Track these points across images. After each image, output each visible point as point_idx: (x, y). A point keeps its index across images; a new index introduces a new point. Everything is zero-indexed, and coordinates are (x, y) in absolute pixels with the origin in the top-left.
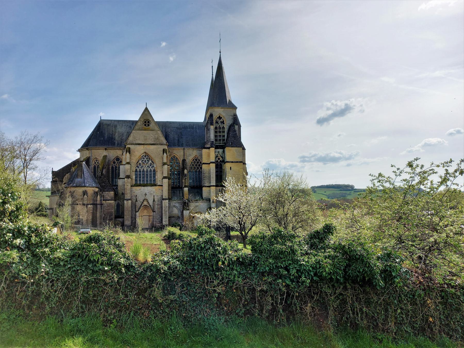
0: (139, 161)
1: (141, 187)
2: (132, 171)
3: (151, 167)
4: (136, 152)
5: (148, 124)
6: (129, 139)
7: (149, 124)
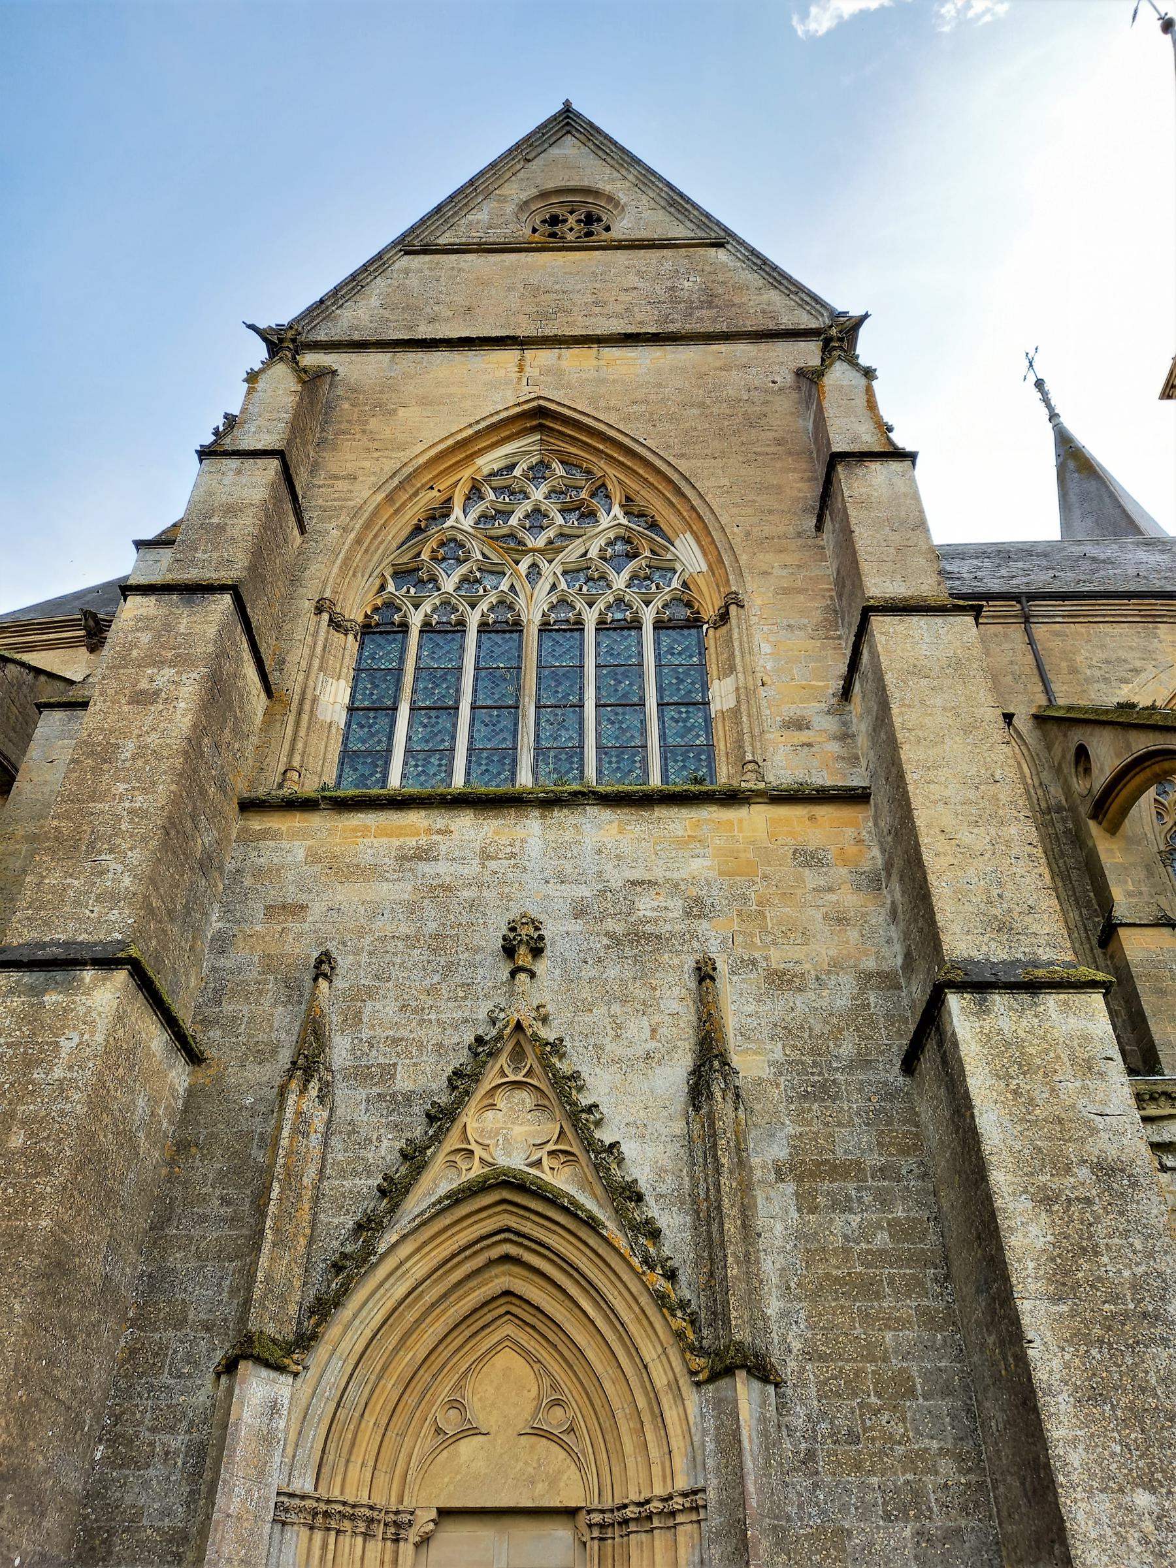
0: (441, 512)
1: (439, 819)
2: (308, 606)
4: (409, 415)
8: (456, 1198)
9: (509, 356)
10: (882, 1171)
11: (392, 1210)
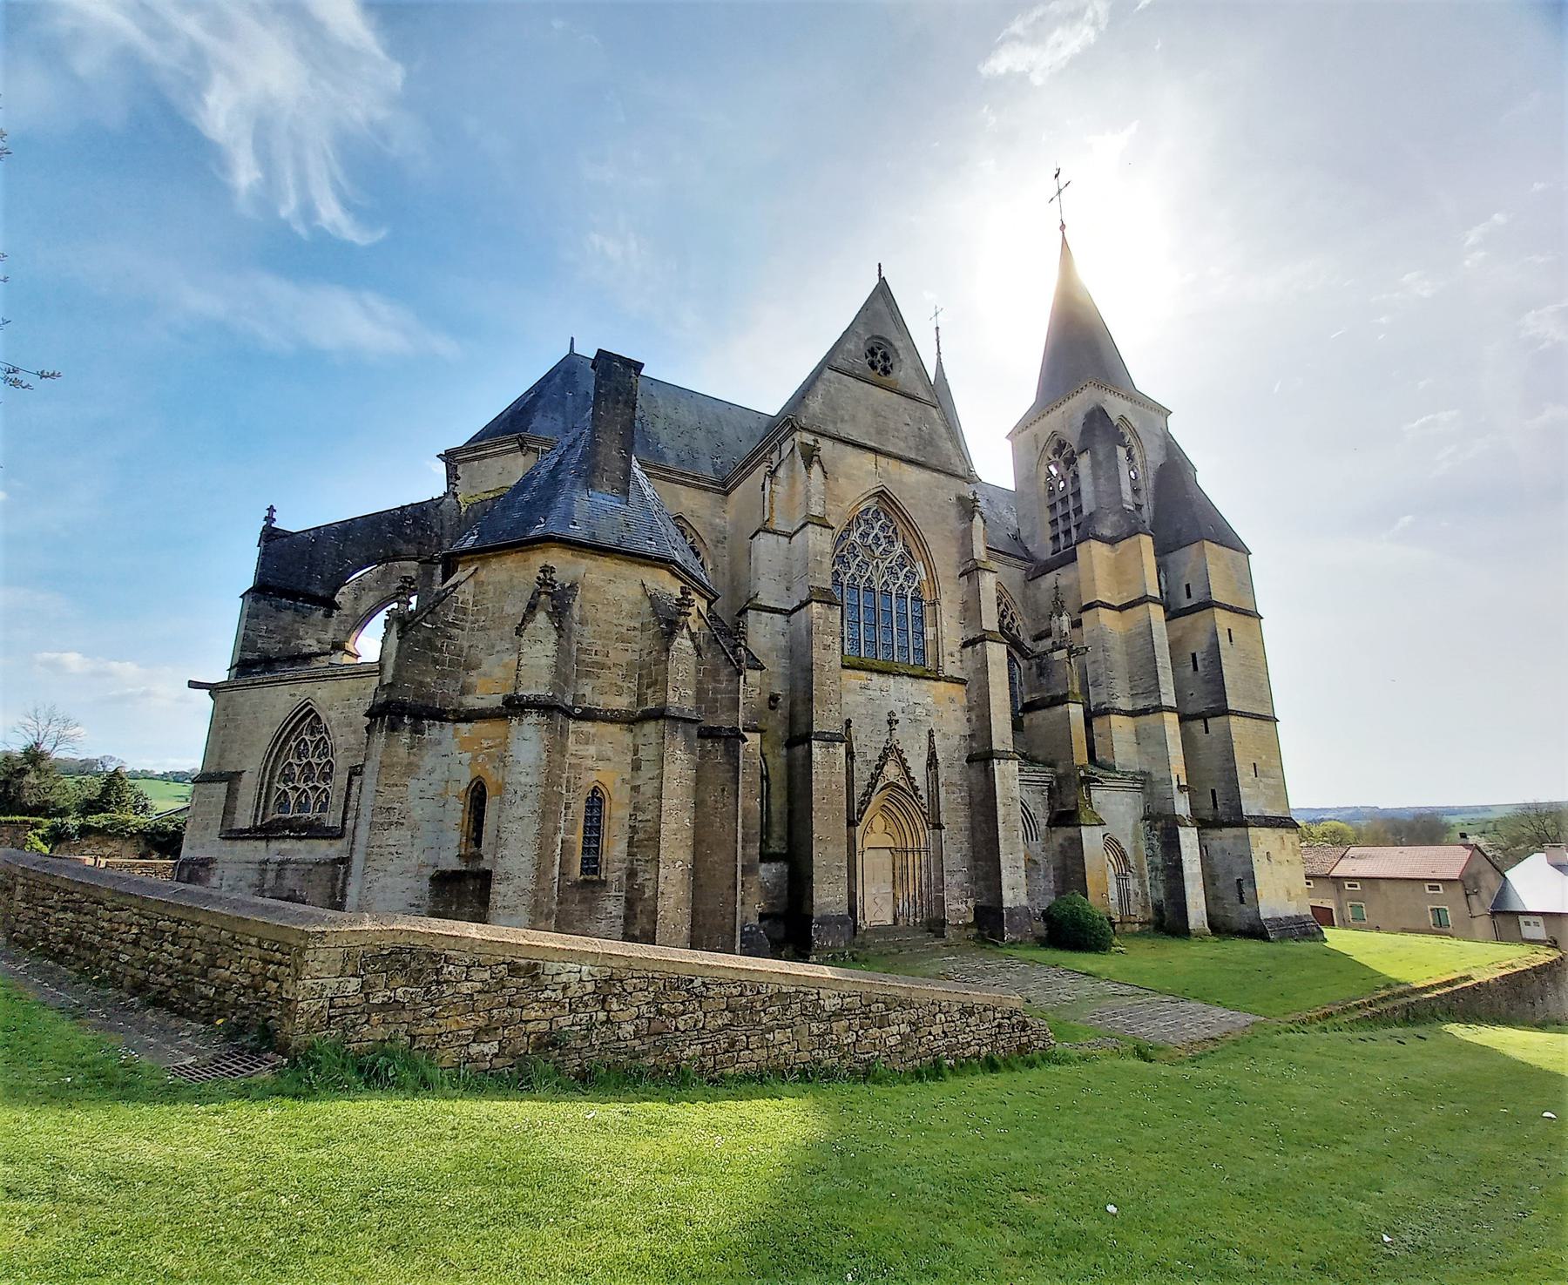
6: (806, 406)
7: (888, 364)
8: (882, 789)
9: (871, 456)
10: (961, 785)
11: (872, 791)
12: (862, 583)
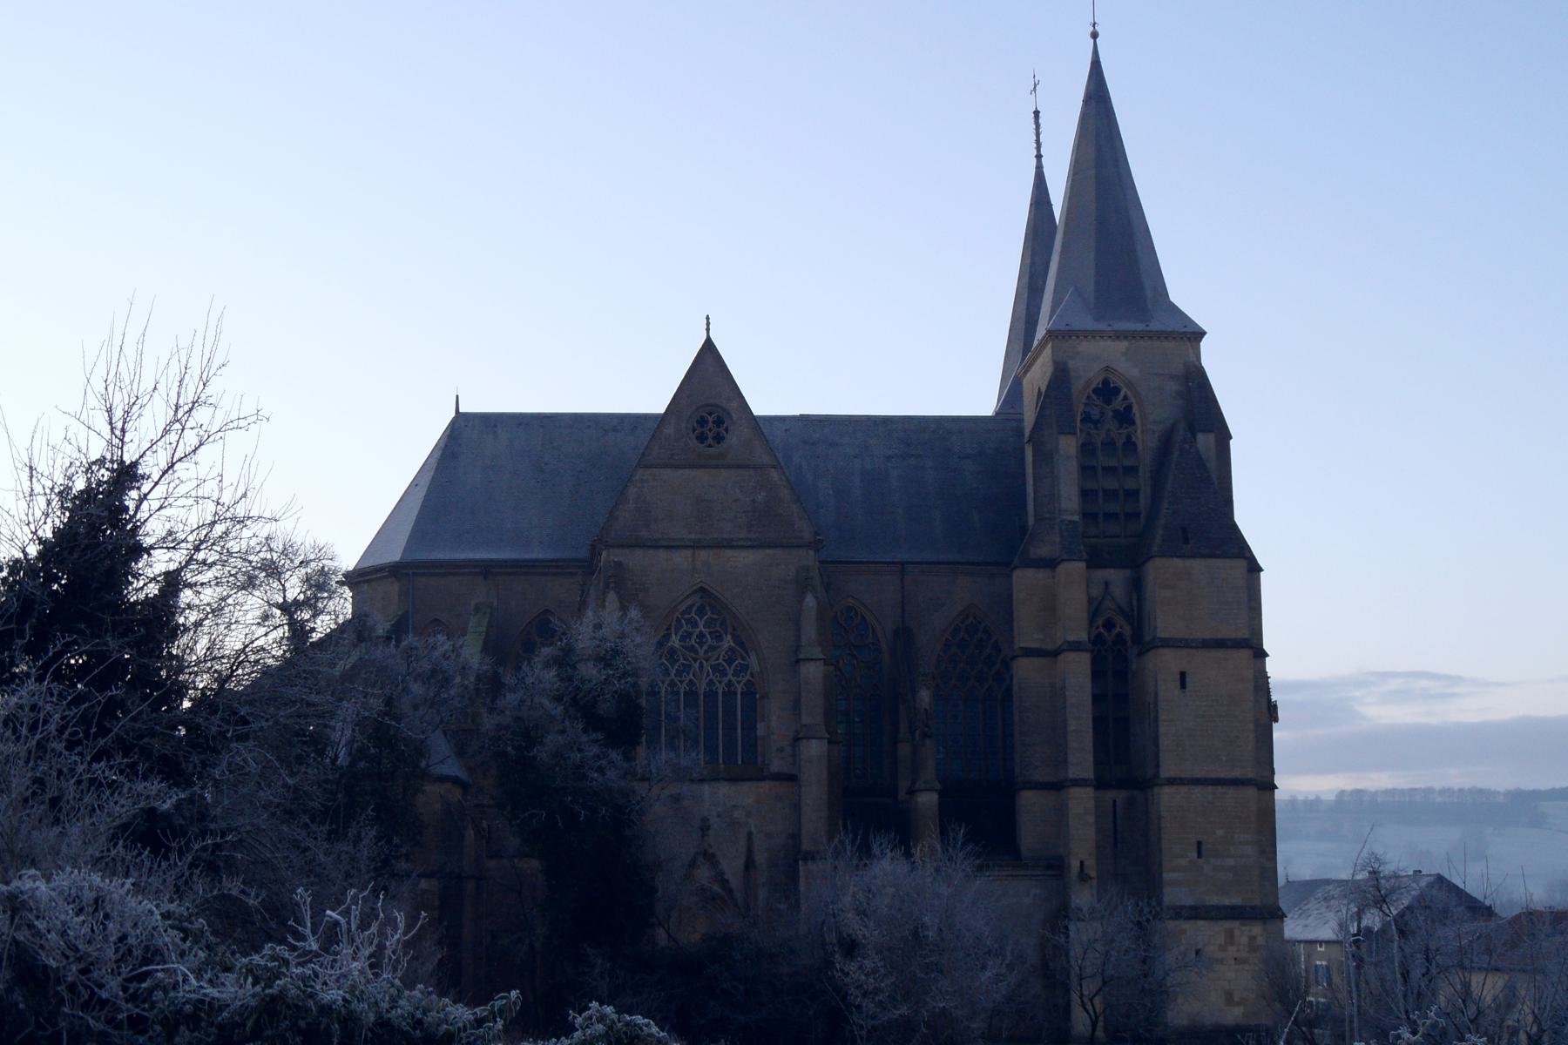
0: (667, 637)
3: (730, 671)
5: (715, 430)
12: (683, 688)
